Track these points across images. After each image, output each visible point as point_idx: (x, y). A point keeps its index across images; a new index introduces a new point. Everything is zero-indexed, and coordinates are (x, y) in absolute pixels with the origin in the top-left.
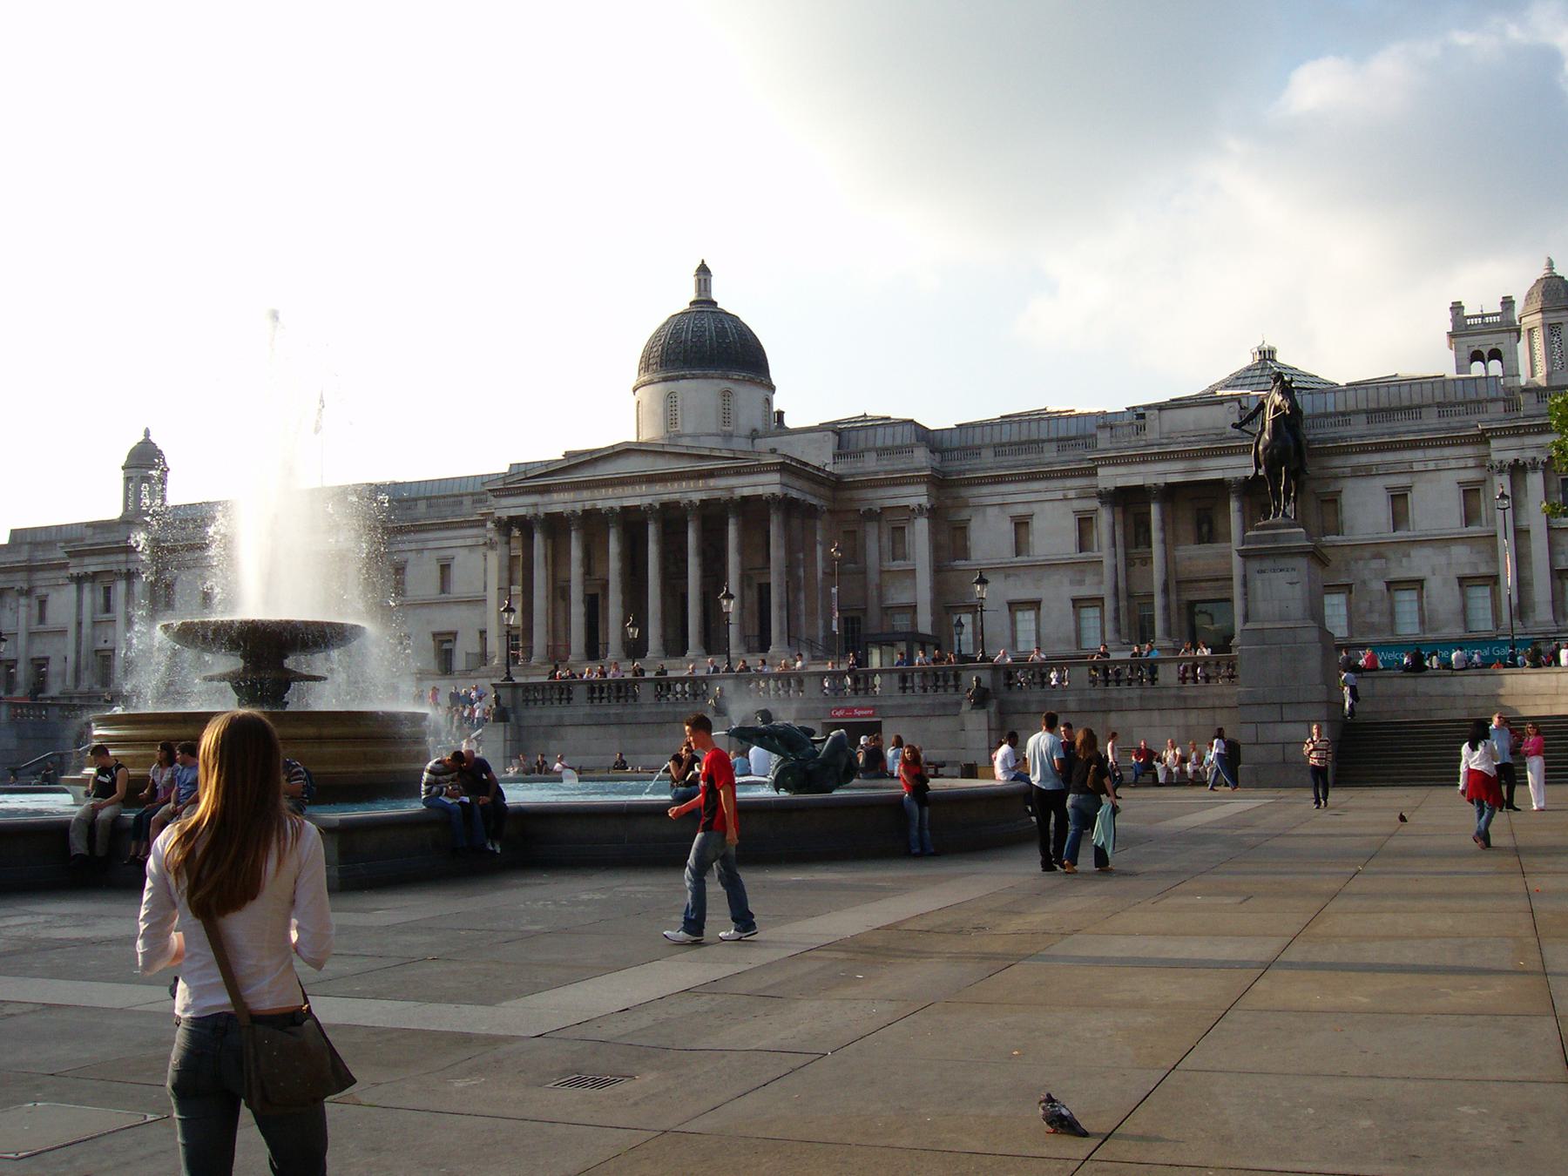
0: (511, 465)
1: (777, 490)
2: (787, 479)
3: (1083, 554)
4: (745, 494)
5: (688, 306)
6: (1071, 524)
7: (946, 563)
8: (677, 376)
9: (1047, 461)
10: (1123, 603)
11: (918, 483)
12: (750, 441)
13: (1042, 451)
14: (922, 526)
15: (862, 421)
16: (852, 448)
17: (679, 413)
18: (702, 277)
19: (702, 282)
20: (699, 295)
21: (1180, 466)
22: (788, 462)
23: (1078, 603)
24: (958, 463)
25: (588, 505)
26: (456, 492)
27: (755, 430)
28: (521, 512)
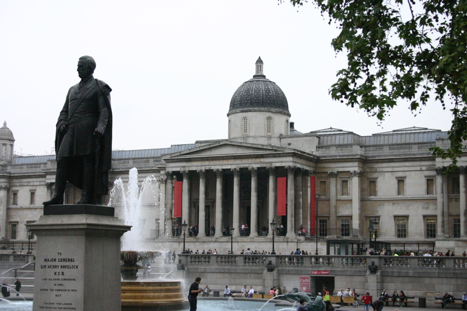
1: (291, 164)
2: (295, 160)
3: (429, 196)
4: (277, 166)
5: (252, 78)
6: (423, 181)
7: (366, 197)
8: (248, 110)
9: (413, 153)
11: (353, 161)
12: (279, 139)
13: (411, 148)
16: (325, 144)
17: (248, 126)
19: (259, 67)
24: (372, 152)
25: (208, 168)
26: (146, 156)
27: (281, 135)
28: (178, 169)
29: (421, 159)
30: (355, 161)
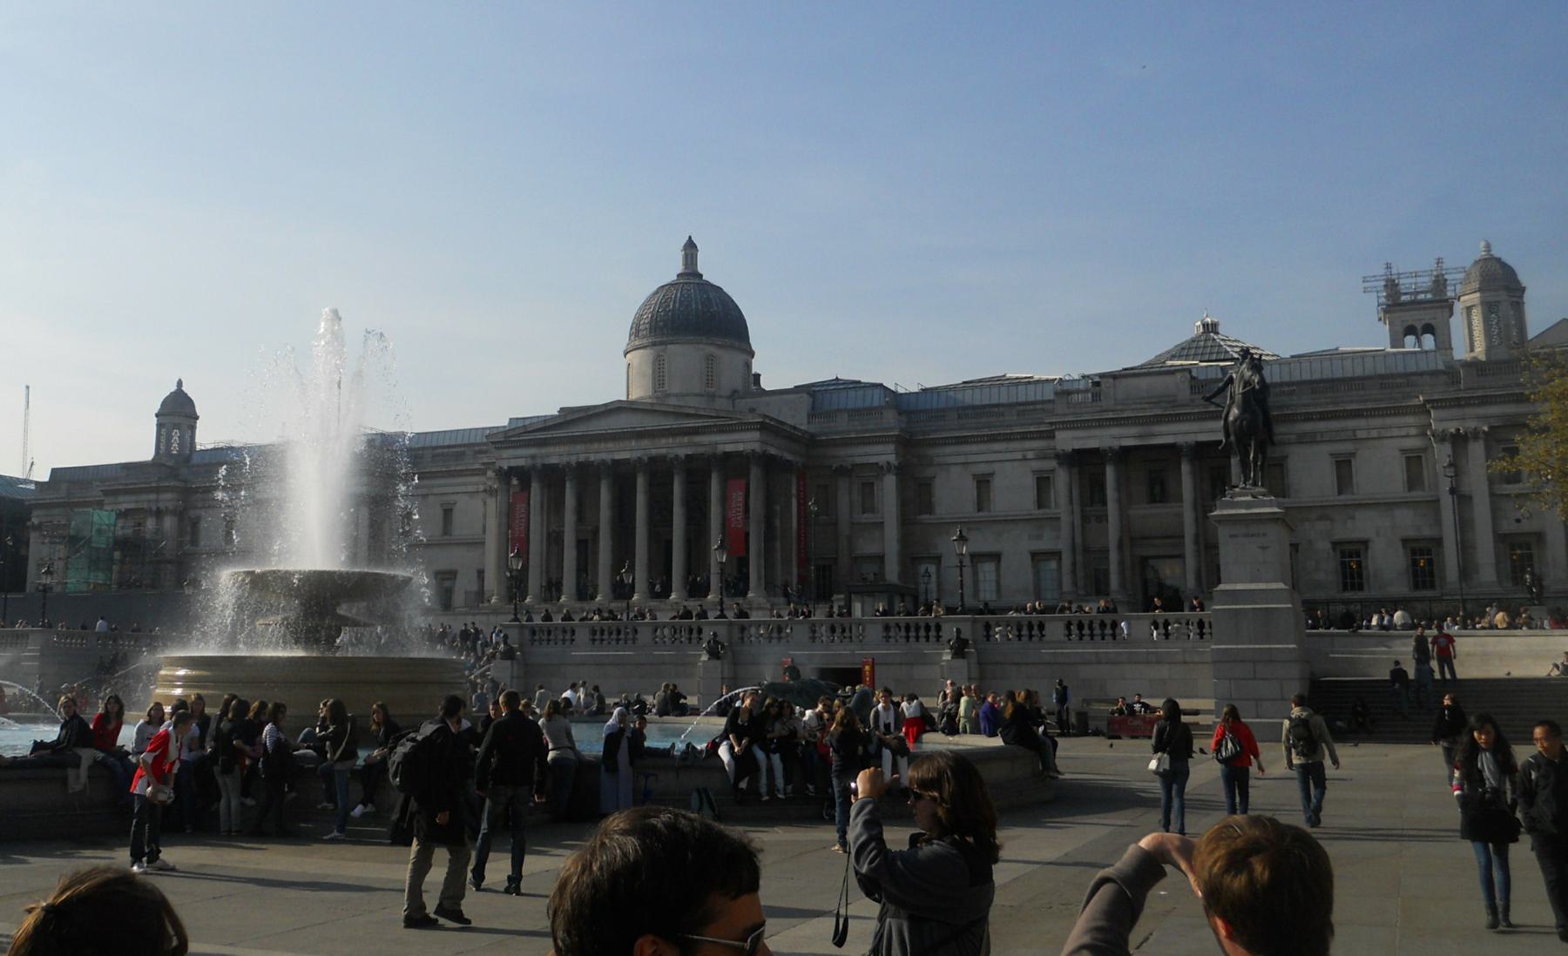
0: (511, 419)
1: (757, 447)
3: (1041, 511)
4: (727, 450)
5: (675, 278)
6: (1030, 481)
10: (1079, 558)
14: (890, 482)
15: (834, 384)
18: (689, 252)
19: (689, 256)
20: (686, 268)
21: (1133, 430)
22: (768, 421)
23: (1036, 556)
25: (582, 458)
27: (735, 391)
28: (521, 462)
29: (1024, 437)
30: (889, 442)
